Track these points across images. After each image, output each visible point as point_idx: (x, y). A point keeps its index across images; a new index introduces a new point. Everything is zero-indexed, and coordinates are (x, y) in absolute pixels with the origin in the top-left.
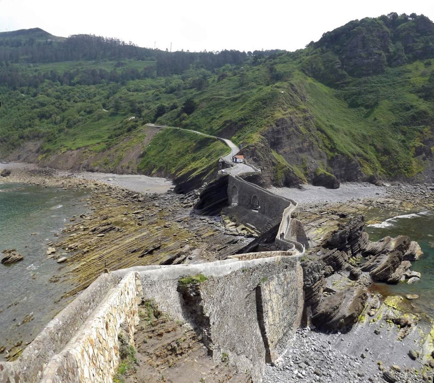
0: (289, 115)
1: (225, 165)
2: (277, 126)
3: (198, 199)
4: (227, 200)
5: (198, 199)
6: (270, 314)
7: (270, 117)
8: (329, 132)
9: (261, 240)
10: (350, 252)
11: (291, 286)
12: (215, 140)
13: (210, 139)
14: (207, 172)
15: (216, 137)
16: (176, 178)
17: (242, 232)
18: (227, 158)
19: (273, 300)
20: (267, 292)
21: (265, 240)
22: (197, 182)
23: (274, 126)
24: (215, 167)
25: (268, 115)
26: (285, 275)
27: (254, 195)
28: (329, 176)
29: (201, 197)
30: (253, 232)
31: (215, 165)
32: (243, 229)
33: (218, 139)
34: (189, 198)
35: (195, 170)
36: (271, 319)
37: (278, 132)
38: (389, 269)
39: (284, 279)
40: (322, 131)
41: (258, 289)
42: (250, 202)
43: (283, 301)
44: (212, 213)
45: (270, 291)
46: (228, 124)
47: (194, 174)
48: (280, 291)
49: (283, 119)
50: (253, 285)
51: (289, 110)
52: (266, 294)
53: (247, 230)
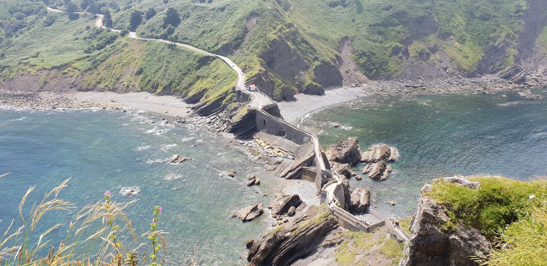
0: (279, 34)
2: (271, 47)
4: (256, 127)
8: (312, 42)
10: (351, 163)
12: (214, 58)
13: (209, 57)
14: (225, 98)
15: (214, 55)
16: (187, 98)
17: (279, 154)
23: (269, 47)
24: (231, 93)
28: (317, 86)
30: (287, 154)
31: (230, 91)
32: (279, 152)
37: (272, 52)
38: (379, 174)
40: (306, 43)
44: (246, 137)
49: (275, 40)
51: (279, 27)
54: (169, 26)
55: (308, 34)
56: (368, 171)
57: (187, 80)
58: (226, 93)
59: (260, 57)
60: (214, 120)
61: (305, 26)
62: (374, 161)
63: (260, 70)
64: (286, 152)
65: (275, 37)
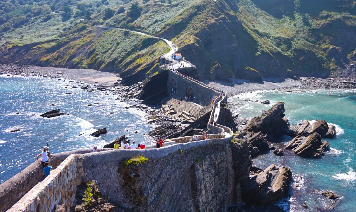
1: (164, 61)
2: (210, 29)
3: (141, 90)
5: (141, 90)
6: (204, 192)
7: (204, 22)
8: (254, 36)
9: (195, 126)
11: (222, 165)
12: (157, 41)
18: (168, 56)
19: (206, 179)
20: (200, 171)
21: (199, 126)
22: (141, 76)
24: (157, 63)
25: (203, 20)
26: (216, 156)
27: (190, 87)
29: (144, 88)
30: (188, 118)
33: (160, 40)
34: (134, 90)
35: (139, 65)
36: (204, 197)
39: (216, 160)
41: (193, 169)
42: (187, 93)
43: (214, 179)
45: (203, 171)
46: (168, 27)
47: (139, 69)
48: (212, 171)
50: (189, 165)
52: (200, 174)
53: (183, 117)
54: (129, 18)
55: (251, 30)
56: (294, 144)
57: (129, 59)
58: (153, 64)
59: (196, 35)
60: (132, 88)
61: (250, 25)
62: (305, 134)
63: (192, 44)
64: (189, 116)
65: (214, 22)
